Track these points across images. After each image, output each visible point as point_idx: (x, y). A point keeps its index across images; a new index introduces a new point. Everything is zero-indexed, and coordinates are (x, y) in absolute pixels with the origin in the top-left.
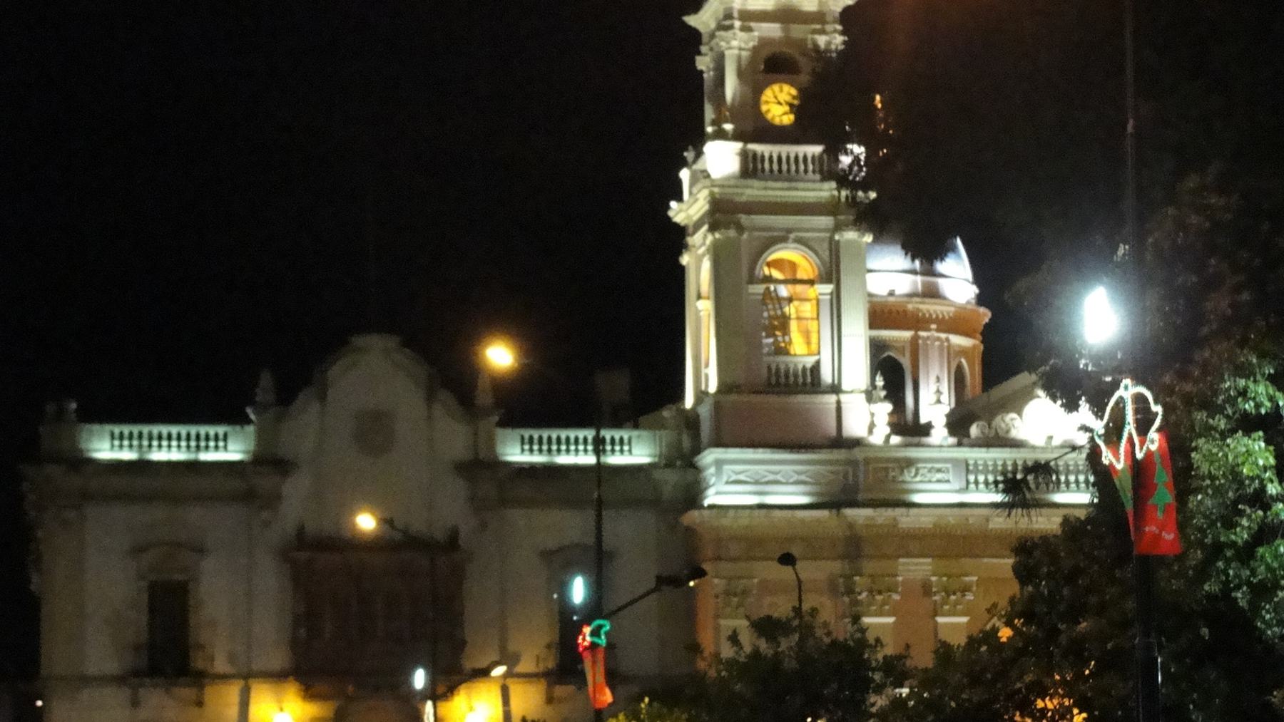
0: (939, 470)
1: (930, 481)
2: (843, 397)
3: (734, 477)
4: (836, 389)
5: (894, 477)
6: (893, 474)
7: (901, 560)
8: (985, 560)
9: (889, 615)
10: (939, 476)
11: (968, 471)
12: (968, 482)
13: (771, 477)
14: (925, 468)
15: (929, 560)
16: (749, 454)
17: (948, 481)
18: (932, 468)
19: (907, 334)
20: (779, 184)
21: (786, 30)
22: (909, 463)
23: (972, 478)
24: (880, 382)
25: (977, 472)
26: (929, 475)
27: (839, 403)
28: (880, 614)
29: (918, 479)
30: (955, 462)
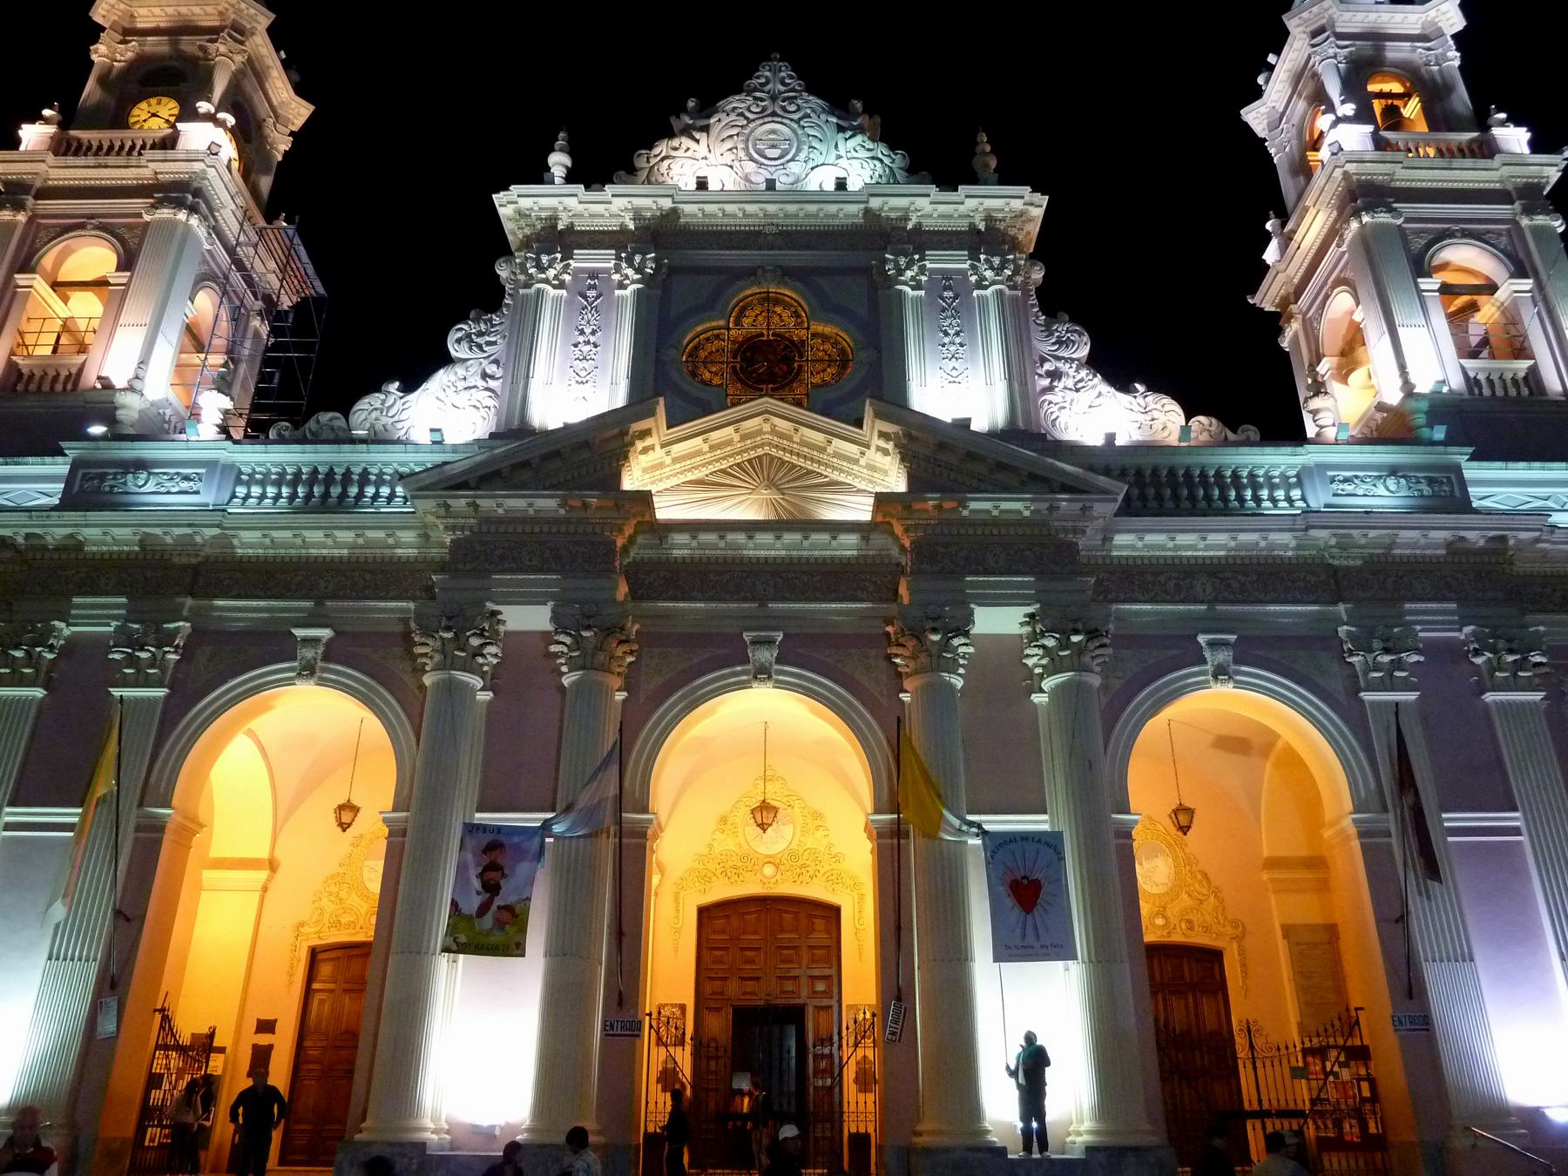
0: (187, 478)
1: (168, 493)
5: (112, 487)
6: (112, 483)
9: (31, 683)
10: (185, 485)
12: (234, 496)
14: (165, 474)
15: (123, 600)
17: (197, 493)
18: (177, 474)
20: (81, 161)
21: (174, 44)
25: (248, 484)
26: (169, 484)
29: (150, 487)
30: (211, 465)
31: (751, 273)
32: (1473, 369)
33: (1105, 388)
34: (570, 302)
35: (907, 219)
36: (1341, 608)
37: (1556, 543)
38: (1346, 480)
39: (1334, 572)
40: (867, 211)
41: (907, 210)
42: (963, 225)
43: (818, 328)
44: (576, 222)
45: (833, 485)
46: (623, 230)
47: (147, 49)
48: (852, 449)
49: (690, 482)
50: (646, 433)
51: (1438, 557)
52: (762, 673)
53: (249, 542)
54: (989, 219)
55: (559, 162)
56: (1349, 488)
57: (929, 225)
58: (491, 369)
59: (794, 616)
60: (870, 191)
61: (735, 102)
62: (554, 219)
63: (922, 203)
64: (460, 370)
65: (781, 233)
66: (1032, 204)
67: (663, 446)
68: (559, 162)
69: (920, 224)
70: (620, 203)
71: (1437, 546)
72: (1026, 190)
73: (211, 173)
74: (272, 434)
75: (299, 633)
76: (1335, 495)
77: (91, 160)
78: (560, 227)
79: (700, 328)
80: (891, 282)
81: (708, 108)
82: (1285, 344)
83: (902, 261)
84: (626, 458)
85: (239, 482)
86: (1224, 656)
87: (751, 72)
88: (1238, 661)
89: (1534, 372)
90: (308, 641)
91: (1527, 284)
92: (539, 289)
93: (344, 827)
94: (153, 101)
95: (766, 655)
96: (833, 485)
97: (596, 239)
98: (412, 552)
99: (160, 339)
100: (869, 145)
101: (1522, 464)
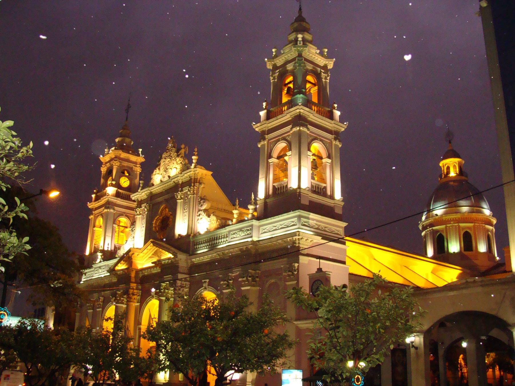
19: (443, 227)
32: (277, 185)
34: (142, 217)
35: (178, 182)
37: (261, 245)
38: (234, 234)
41: (177, 180)
44: (142, 198)
47: (108, 166)
49: (149, 257)
50: (133, 254)
51: (239, 253)
52: (153, 297)
54: (190, 177)
56: (234, 236)
57: (184, 180)
60: (176, 176)
65: (166, 190)
66: (195, 171)
67: (142, 252)
69: (182, 181)
71: (237, 251)
73: (110, 199)
76: (232, 238)
78: (140, 200)
79: (156, 218)
83: (177, 194)
84: (132, 259)
92: (136, 217)
99: (107, 238)
100: (181, 159)
101: (269, 219)
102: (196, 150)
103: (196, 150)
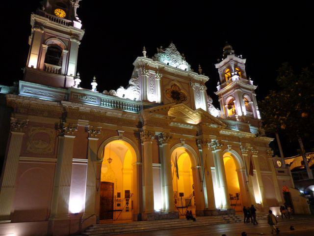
0: (93, 99)
2: (67, 77)
3: (27, 91)
4: (66, 75)
7: (79, 120)
8: (105, 124)
9: (73, 135)
10: (93, 100)
11: (101, 101)
13: (40, 93)
15: (88, 121)
16: (33, 85)
20: (55, 23)
22: (85, 95)
23: (102, 103)
24: (78, 74)
25: (104, 101)
27: (66, 78)
28: (70, 134)
29: (87, 99)
30: (97, 97)
31: (173, 80)
33: (214, 108)
36: (240, 143)
39: (239, 138)
40: (189, 75)
42: (199, 80)
43: (182, 91)
45: (188, 118)
46: (156, 68)
48: (192, 113)
53: (109, 114)
55: (145, 52)
58: (138, 88)
59: (186, 137)
61: (168, 49)
62: (147, 64)
63: (196, 76)
64: (133, 87)
68: (145, 52)
70: (157, 64)
72: (208, 77)
74: (104, 92)
75: (119, 131)
77: (57, 24)
80: (192, 87)
81: (164, 49)
82: (219, 101)
85: (101, 101)
86: (230, 148)
87: (169, 45)
88: (232, 149)
89: (253, 114)
90: (120, 133)
91: (252, 102)
93: (110, 162)
94: (59, 10)
95: (183, 142)
96: (188, 118)
97: (152, 69)
98: (134, 119)
102: (200, 66)
103: (200, 66)
